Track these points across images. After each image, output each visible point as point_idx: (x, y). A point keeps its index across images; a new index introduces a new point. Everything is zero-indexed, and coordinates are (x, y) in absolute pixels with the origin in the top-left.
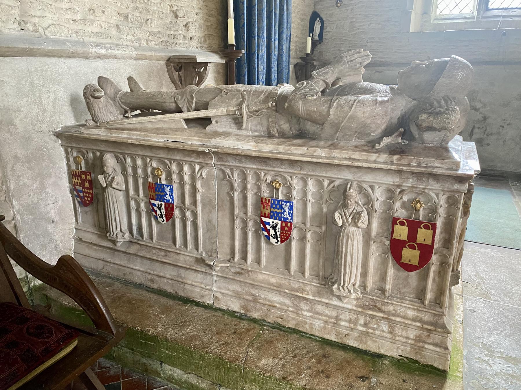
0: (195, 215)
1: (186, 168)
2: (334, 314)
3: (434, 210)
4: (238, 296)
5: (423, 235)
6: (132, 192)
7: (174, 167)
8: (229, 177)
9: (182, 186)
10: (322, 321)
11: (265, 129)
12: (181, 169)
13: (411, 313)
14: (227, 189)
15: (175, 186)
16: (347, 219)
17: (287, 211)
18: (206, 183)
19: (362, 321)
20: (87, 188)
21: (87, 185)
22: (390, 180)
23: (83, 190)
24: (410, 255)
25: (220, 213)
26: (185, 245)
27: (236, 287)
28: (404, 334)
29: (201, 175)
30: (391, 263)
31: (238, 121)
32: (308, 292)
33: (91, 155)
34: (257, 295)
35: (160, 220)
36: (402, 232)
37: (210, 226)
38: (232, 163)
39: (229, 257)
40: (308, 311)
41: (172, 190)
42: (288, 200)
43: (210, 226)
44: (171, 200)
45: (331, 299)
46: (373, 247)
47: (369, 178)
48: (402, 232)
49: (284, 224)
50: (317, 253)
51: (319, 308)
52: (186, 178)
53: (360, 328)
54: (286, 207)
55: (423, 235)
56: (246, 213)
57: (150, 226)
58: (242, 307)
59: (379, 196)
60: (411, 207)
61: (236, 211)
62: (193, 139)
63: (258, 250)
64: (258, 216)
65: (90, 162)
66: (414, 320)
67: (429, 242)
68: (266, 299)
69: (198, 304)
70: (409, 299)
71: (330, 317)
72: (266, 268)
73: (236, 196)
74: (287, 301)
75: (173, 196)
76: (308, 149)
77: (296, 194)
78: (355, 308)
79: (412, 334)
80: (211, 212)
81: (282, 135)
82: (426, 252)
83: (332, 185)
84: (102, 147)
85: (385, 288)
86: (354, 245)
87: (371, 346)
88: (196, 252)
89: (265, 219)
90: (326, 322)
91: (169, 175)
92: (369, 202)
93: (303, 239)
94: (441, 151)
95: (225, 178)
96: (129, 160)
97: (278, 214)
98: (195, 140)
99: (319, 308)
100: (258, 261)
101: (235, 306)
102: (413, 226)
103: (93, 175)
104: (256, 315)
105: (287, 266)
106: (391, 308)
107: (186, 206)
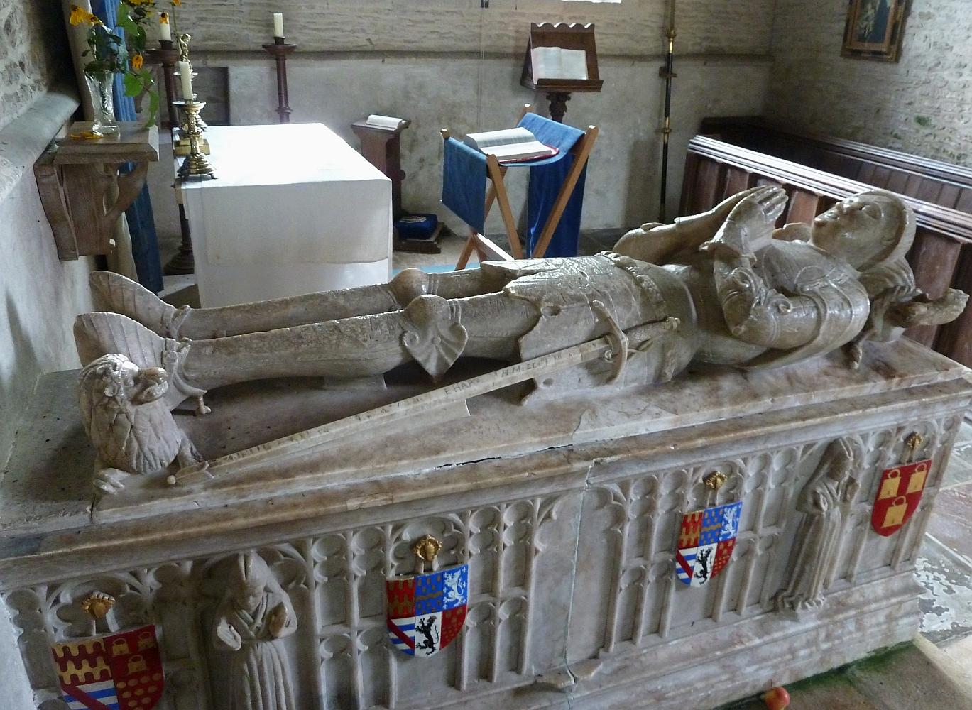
0: (519, 607)
2: (786, 646)
6: (320, 623)
8: (617, 498)
10: (768, 669)
11: (652, 371)
12: (491, 520)
15: (473, 566)
16: (834, 500)
17: (730, 521)
19: (823, 635)
20: (137, 676)
23: (121, 685)
25: (583, 575)
26: (485, 672)
28: (874, 621)
29: (548, 516)
32: (747, 636)
33: (150, 580)
34: (659, 687)
39: (590, 652)
40: (748, 665)
41: (464, 577)
42: (732, 500)
44: (460, 599)
45: (783, 628)
49: (722, 546)
50: (765, 568)
52: (506, 538)
53: (825, 646)
56: (644, 555)
61: (624, 562)
63: (660, 608)
64: (669, 550)
65: (148, 597)
66: (887, 597)
68: (677, 687)
70: (876, 571)
71: (782, 655)
73: (628, 531)
74: (713, 669)
75: (465, 589)
76: (773, 401)
78: (819, 623)
79: (881, 618)
80: (558, 582)
82: (913, 500)
83: (809, 453)
85: (852, 572)
88: (514, 676)
89: (684, 553)
91: (455, 546)
96: (316, 552)
97: (712, 532)
98: (531, 444)
100: (657, 629)
103: (158, 632)
106: (856, 597)
107: (500, 595)
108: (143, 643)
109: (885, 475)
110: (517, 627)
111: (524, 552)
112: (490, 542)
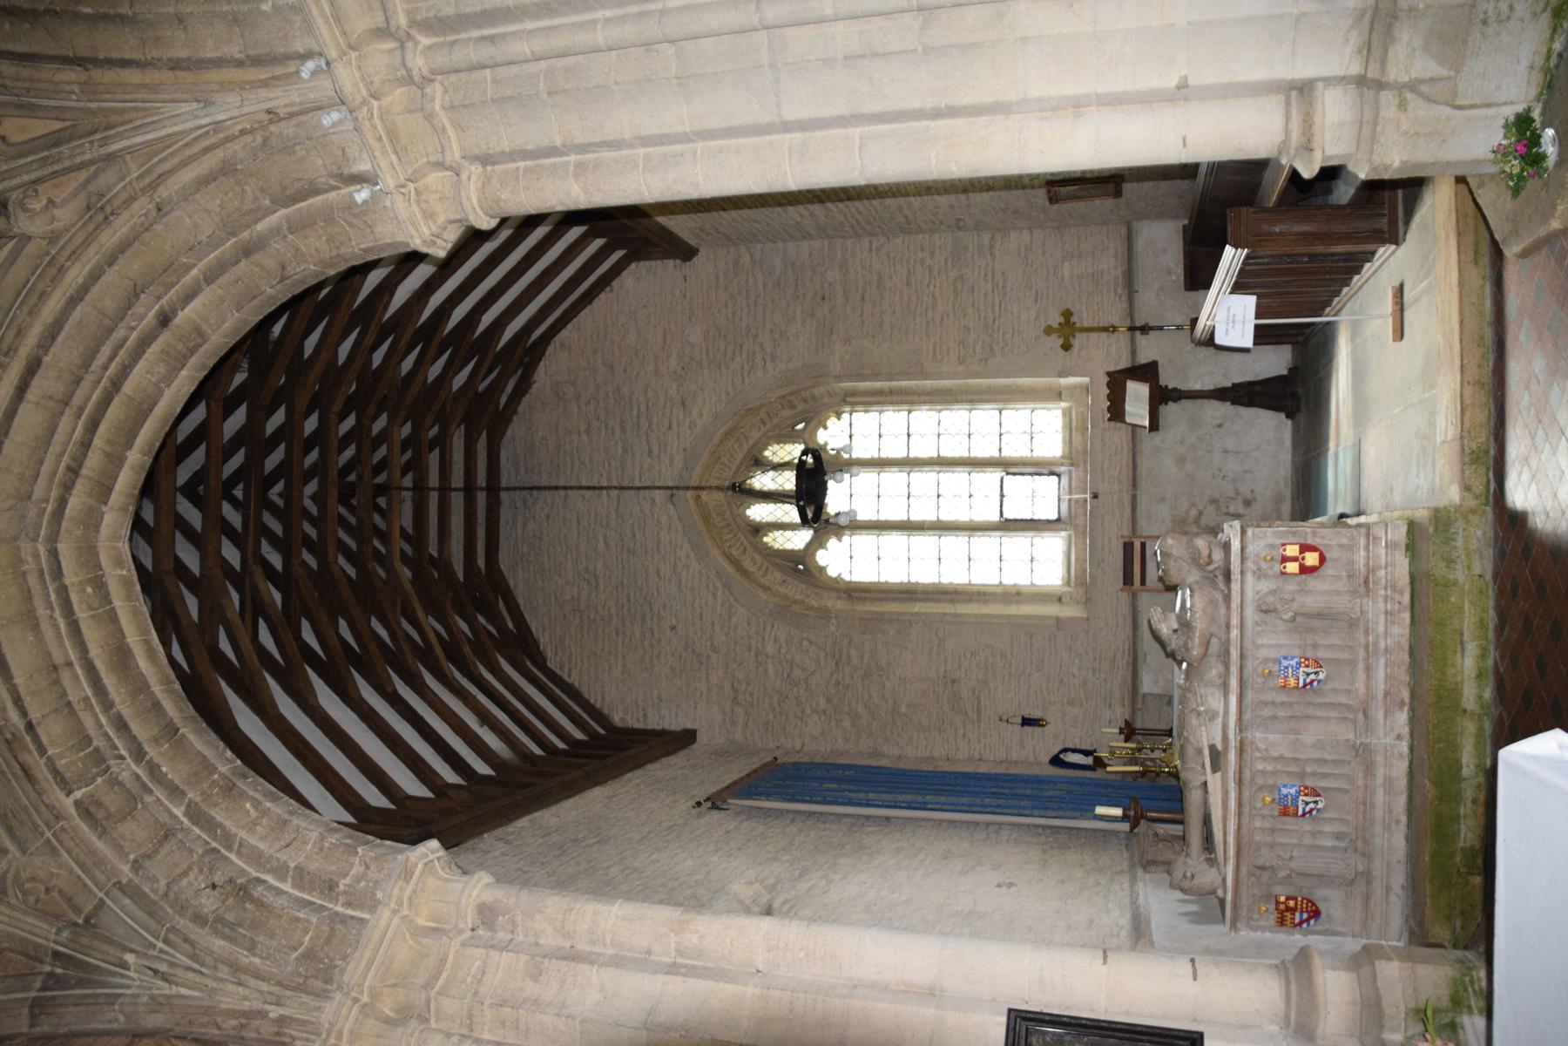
1: (1260, 767)
2: (1382, 617)
5: (1292, 551)
7: (1260, 781)
13: (1362, 553)
21: (1292, 903)
22: (1249, 578)
24: (1311, 559)
30: (1320, 572)
35: (1320, 805)
36: (1292, 567)
38: (1247, 716)
47: (1250, 595)
48: (1292, 567)
51: (1381, 629)
52: (1270, 768)
54: (1285, 663)
55: (1292, 551)
57: (1330, 820)
58: (1401, 709)
59: (1265, 586)
62: (1232, 756)
67: (1297, 547)
69: (1411, 763)
72: (1352, 683)
77: (1272, 654)
86: (1311, 603)
87: (1404, 581)
90: (1393, 623)
100: (1348, 692)
101: (1402, 717)
102: (1285, 559)
104: (1406, 694)
108: (1282, 899)
109: (1283, 574)
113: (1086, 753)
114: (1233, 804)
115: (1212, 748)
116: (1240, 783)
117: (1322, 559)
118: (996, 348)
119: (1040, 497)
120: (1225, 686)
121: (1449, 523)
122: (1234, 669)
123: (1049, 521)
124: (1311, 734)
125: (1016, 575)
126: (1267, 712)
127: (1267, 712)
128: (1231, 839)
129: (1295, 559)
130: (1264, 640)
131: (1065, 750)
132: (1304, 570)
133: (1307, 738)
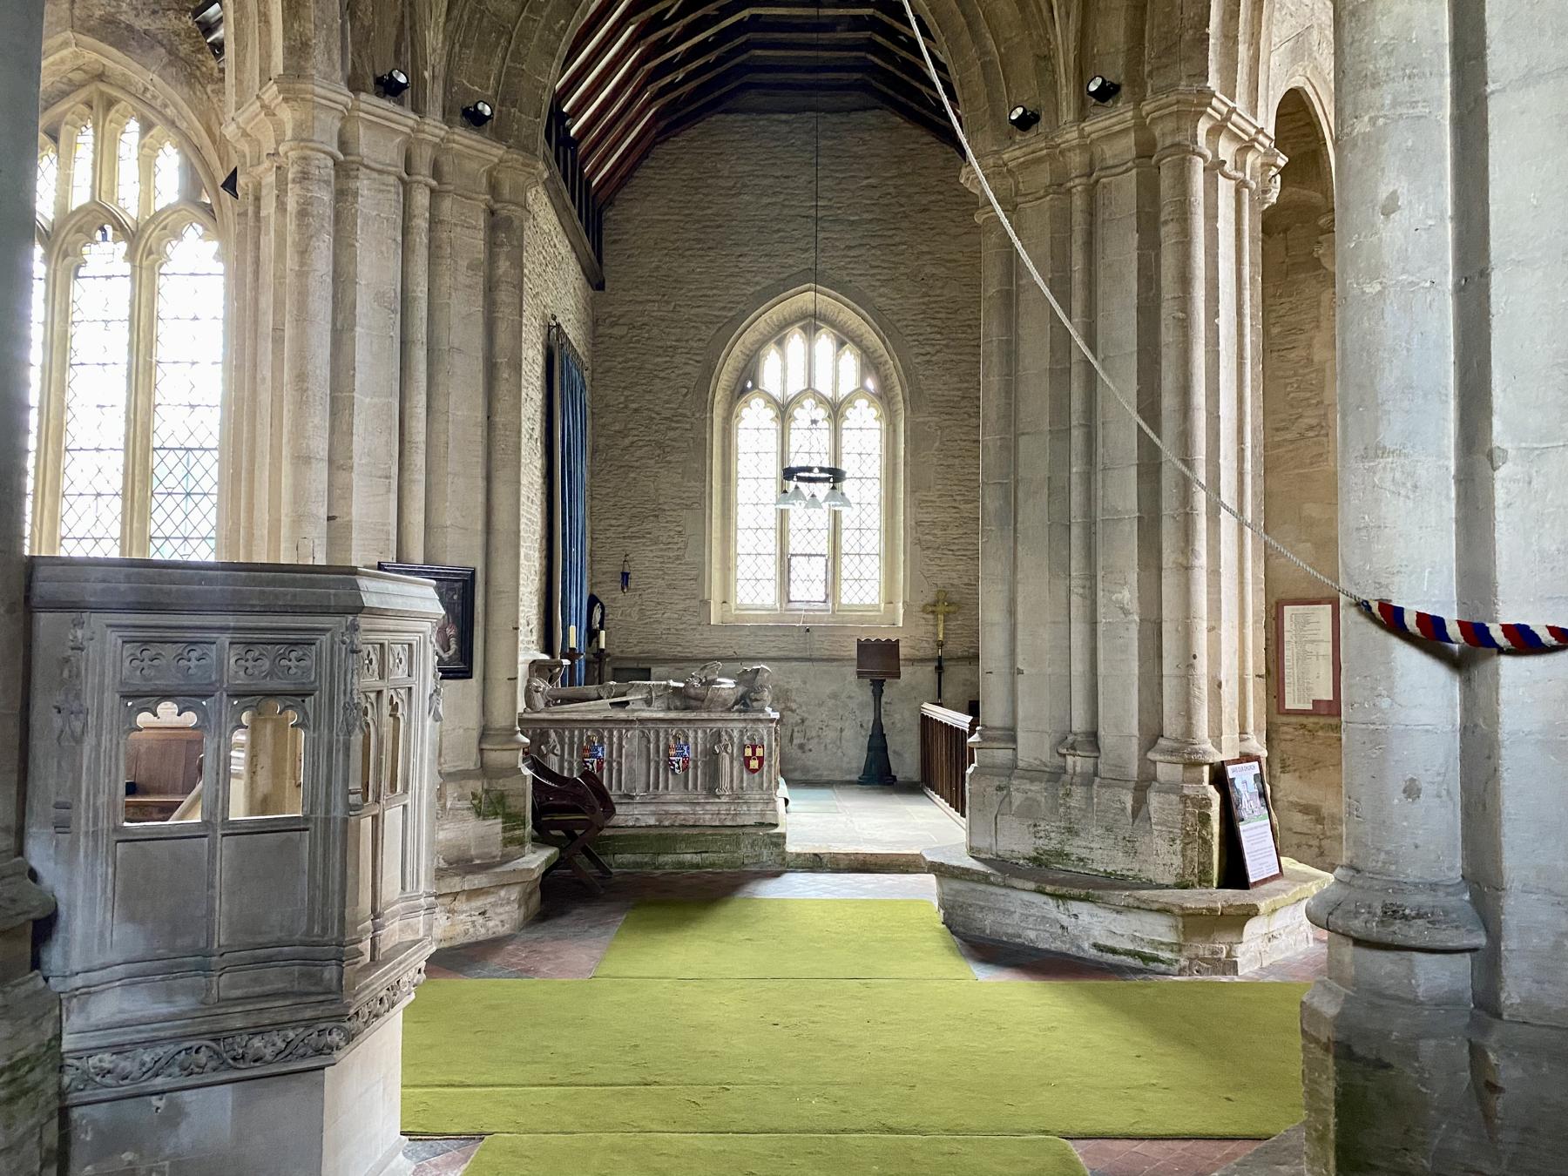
0: (620, 764)
3: (762, 739)
4: (654, 813)
5: (759, 752)
9: (611, 744)
14: (644, 742)
18: (630, 740)
22: (741, 725)
24: (754, 764)
27: (652, 808)
31: (648, 702)
36: (748, 752)
37: (631, 770)
42: (686, 743)
43: (631, 770)
46: (735, 764)
47: (731, 725)
50: (704, 774)
59: (736, 734)
60: (752, 738)
62: (622, 715)
81: (676, 709)
82: (761, 760)
84: (545, 725)
92: (731, 738)
93: (696, 767)
94: (762, 711)
95: (644, 735)
99: (708, 807)
101: (652, 821)
102: (754, 748)
105: (686, 787)
110: (619, 771)
111: (620, 747)
112: (611, 738)
113: (601, 623)
114: (591, 716)
115: (627, 703)
116: (605, 721)
117: (754, 771)
118: (928, 552)
119: (808, 587)
120: (669, 709)
121: (777, 845)
122: (681, 715)
123: (788, 594)
124: (639, 765)
125: (744, 567)
126: (652, 736)
127: (652, 736)
128: (566, 716)
129: (754, 752)
130: (700, 734)
131: (603, 607)
132: (747, 760)
133: (636, 764)
